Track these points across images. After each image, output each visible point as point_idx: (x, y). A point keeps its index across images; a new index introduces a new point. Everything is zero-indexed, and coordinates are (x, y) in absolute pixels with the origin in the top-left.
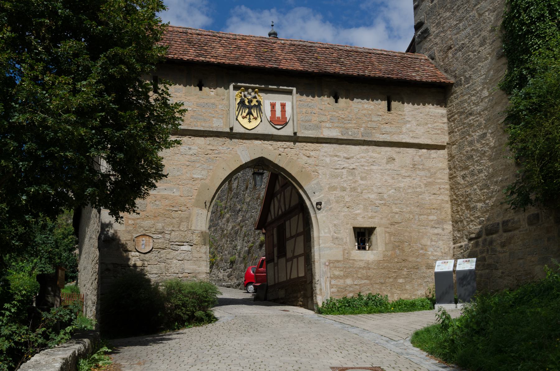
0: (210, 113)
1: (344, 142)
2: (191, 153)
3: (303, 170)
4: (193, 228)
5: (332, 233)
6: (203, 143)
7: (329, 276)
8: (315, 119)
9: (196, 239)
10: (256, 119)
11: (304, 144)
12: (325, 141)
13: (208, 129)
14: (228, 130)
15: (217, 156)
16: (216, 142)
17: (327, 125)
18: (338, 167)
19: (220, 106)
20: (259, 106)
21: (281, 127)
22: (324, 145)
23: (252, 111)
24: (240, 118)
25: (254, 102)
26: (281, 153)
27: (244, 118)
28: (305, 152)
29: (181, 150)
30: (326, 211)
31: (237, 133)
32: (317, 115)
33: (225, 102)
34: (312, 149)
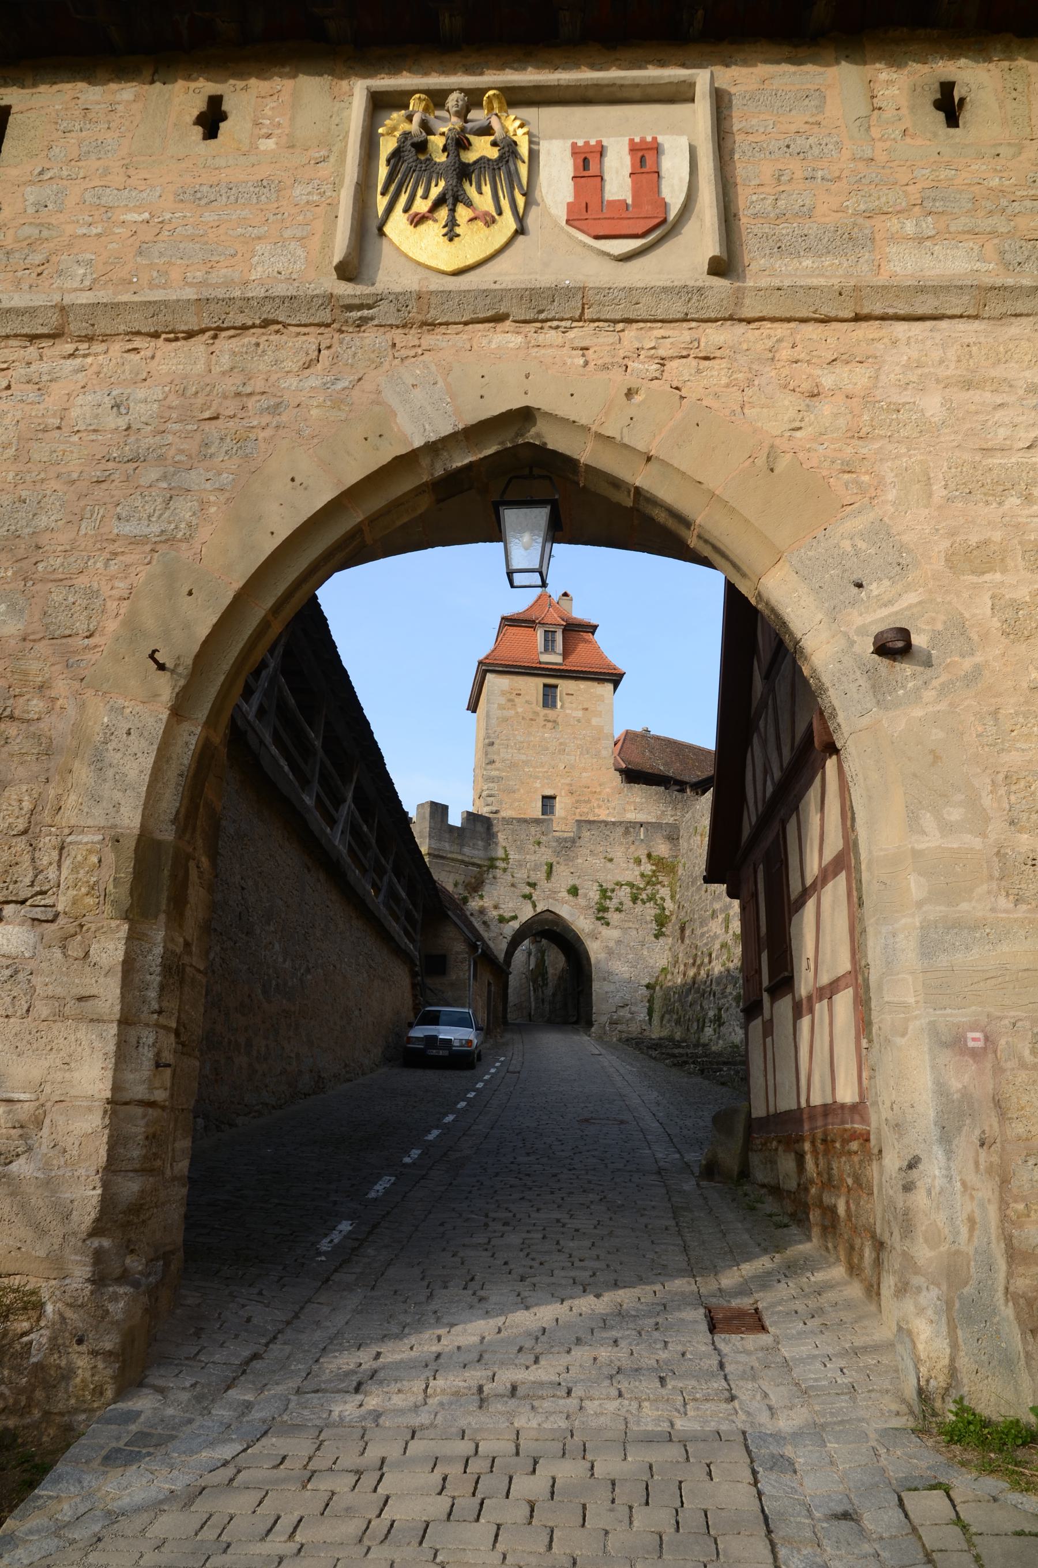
3: (783, 464)
5: (997, 829)
6: (200, 367)
11: (780, 330)
13: (220, 293)
24: (397, 226)
29: (74, 413)
30: (944, 691)
33: (325, 170)
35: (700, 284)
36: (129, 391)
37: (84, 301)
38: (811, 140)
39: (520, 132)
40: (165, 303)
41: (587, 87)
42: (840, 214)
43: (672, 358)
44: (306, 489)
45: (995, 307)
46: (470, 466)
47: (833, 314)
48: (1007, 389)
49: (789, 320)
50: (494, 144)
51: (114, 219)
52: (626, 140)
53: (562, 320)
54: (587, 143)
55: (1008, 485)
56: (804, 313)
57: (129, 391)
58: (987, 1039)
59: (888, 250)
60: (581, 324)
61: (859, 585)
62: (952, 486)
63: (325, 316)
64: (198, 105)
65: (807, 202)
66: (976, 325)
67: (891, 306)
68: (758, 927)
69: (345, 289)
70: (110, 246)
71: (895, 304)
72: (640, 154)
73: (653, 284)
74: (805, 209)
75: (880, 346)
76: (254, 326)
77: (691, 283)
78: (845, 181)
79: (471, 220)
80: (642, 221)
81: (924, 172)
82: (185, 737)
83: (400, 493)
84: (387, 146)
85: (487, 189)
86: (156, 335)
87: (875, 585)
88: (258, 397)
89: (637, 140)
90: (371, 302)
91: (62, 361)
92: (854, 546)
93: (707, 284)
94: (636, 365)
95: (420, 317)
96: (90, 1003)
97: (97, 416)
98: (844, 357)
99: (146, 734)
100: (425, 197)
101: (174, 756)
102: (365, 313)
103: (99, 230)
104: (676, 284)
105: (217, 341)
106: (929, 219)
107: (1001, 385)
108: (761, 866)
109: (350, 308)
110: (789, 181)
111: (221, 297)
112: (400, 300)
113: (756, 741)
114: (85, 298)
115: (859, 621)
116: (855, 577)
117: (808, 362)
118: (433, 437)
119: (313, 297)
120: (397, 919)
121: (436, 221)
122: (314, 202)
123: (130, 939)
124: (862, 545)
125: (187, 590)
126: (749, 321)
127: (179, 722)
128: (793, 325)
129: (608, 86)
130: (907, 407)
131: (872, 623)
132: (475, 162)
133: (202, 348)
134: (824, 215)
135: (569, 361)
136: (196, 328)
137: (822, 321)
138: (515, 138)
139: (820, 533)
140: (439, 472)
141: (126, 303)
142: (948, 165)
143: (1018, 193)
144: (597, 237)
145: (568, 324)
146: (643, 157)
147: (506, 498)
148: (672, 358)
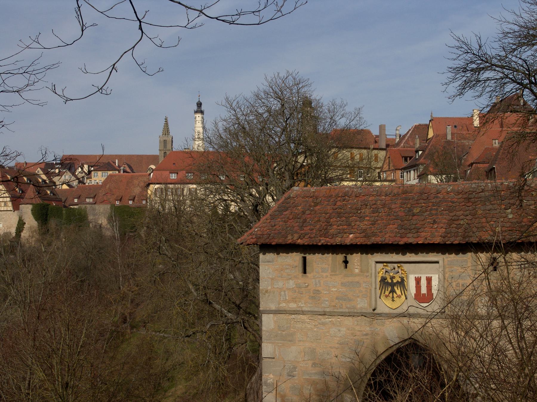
10: (399, 297)
20: (402, 283)
25: (397, 279)
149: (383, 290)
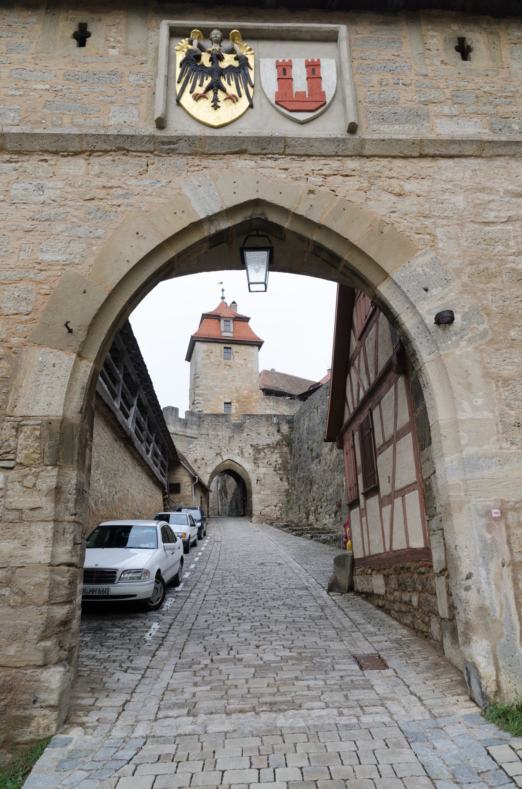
0: (102, 93)
1: (501, 151)
2: (42, 198)
3: (386, 230)
4: (20, 411)
6: (82, 171)
7: (507, 559)
8: (408, 98)
9: (26, 445)
11: (384, 162)
12: (443, 151)
13: (92, 131)
14: (151, 129)
15: (120, 201)
16: (121, 168)
17: (446, 110)
18: (491, 216)
19: (132, 78)
21: (310, 115)
22: (442, 163)
23: (224, 83)
24: (187, 100)
25: (228, 61)
26: (313, 188)
27: (197, 98)
28: (386, 183)
29: (13, 192)
31: (179, 139)
32: (412, 87)
33: (146, 68)
34: (408, 175)
35: (344, 137)
36: (43, 182)
37: (15, 132)
38: (397, 64)
39: (249, 52)
40: (61, 135)
41: (282, 31)
42: (412, 103)
43: (330, 175)
44: (144, 238)
45: (488, 152)
46: (228, 229)
47: (409, 154)
48: (495, 192)
49: (387, 157)
50: (236, 59)
51: (29, 87)
52: (304, 60)
53: (274, 154)
54: (284, 61)
55: (497, 240)
56: (395, 153)
57: (43, 182)
58: (502, 512)
59: (436, 121)
60: (283, 156)
61: (426, 290)
62: (470, 240)
63: (151, 147)
64: (73, 28)
65: (395, 96)
66: (479, 161)
67: (438, 150)
68: (356, 463)
69: (159, 133)
70: (28, 102)
71: (440, 149)
72: (312, 68)
73: (320, 136)
74: (394, 100)
75: (431, 170)
76: (111, 150)
77: (339, 136)
78: (414, 85)
79: (225, 99)
80: (314, 103)
81: (452, 82)
82: (85, 368)
83: (193, 242)
84: (180, 57)
85: (233, 83)
86: (56, 153)
87: (434, 289)
88: (116, 189)
89: (310, 60)
90: (174, 140)
91: (3, 164)
92: (423, 270)
93: (348, 137)
94: (312, 178)
95: (201, 150)
96: (37, 512)
97: (24, 196)
98: (414, 176)
99: (64, 366)
100: (201, 85)
101: (79, 378)
102: (172, 146)
103: (21, 93)
104: (332, 136)
105: (91, 158)
106: (456, 106)
107: (491, 190)
108: (357, 433)
109: (163, 143)
110: (386, 85)
111: (93, 133)
112: (190, 140)
113: (352, 371)
114: (15, 130)
115: (427, 308)
116: (424, 286)
117: (397, 178)
118: (211, 214)
119: (144, 136)
120: (157, 465)
121: (207, 99)
122: (141, 85)
123: (59, 475)
124: (427, 270)
125: (83, 290)
126: (368, 157)
127: (81, 360)
128: (389, 159)
129: (293, 31)
130: (447, 201)
131: (433, 309)
132: (227, 68)
133: (83, 161)
134: (405, 103)
135: (278, 175)
136: (79, 150)
137: (403, 157)
138: (247, 56)
139: (406, 264)
140: (213, 231)
141: (40, 134)
142: (463, 79)
143: (498, 95)
144: (291, 111)
145: (277, 156)
146: (313, 69)
147: (245, 246)
148: (330, 175)
149: (189, 86)
